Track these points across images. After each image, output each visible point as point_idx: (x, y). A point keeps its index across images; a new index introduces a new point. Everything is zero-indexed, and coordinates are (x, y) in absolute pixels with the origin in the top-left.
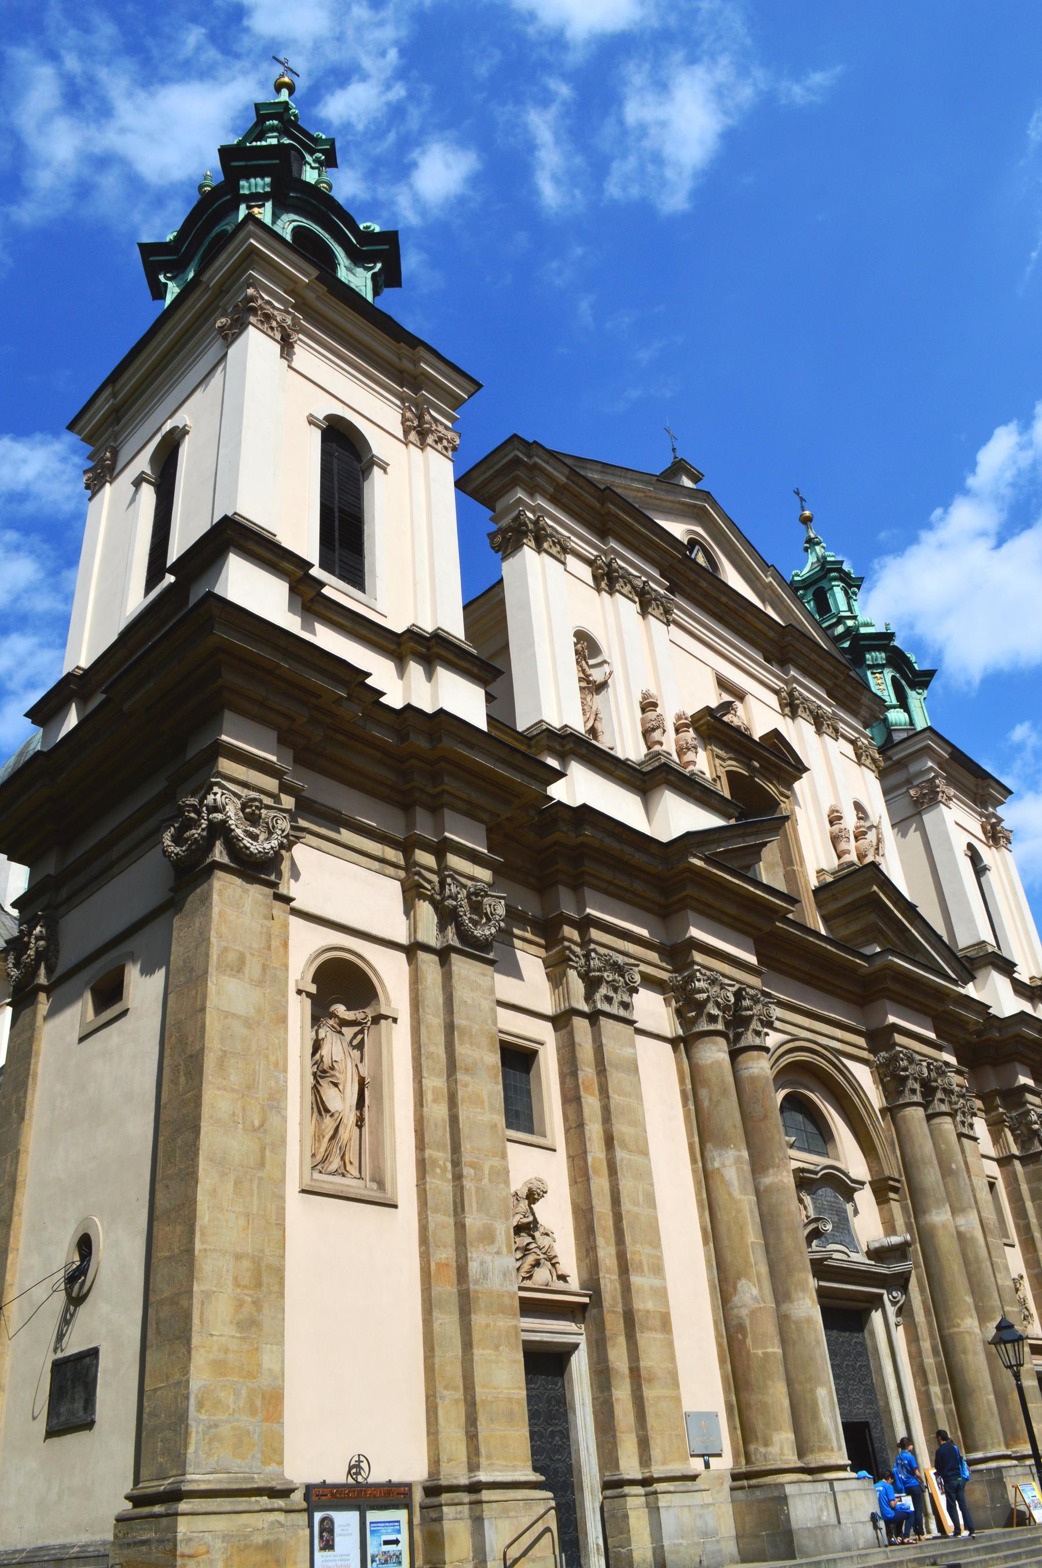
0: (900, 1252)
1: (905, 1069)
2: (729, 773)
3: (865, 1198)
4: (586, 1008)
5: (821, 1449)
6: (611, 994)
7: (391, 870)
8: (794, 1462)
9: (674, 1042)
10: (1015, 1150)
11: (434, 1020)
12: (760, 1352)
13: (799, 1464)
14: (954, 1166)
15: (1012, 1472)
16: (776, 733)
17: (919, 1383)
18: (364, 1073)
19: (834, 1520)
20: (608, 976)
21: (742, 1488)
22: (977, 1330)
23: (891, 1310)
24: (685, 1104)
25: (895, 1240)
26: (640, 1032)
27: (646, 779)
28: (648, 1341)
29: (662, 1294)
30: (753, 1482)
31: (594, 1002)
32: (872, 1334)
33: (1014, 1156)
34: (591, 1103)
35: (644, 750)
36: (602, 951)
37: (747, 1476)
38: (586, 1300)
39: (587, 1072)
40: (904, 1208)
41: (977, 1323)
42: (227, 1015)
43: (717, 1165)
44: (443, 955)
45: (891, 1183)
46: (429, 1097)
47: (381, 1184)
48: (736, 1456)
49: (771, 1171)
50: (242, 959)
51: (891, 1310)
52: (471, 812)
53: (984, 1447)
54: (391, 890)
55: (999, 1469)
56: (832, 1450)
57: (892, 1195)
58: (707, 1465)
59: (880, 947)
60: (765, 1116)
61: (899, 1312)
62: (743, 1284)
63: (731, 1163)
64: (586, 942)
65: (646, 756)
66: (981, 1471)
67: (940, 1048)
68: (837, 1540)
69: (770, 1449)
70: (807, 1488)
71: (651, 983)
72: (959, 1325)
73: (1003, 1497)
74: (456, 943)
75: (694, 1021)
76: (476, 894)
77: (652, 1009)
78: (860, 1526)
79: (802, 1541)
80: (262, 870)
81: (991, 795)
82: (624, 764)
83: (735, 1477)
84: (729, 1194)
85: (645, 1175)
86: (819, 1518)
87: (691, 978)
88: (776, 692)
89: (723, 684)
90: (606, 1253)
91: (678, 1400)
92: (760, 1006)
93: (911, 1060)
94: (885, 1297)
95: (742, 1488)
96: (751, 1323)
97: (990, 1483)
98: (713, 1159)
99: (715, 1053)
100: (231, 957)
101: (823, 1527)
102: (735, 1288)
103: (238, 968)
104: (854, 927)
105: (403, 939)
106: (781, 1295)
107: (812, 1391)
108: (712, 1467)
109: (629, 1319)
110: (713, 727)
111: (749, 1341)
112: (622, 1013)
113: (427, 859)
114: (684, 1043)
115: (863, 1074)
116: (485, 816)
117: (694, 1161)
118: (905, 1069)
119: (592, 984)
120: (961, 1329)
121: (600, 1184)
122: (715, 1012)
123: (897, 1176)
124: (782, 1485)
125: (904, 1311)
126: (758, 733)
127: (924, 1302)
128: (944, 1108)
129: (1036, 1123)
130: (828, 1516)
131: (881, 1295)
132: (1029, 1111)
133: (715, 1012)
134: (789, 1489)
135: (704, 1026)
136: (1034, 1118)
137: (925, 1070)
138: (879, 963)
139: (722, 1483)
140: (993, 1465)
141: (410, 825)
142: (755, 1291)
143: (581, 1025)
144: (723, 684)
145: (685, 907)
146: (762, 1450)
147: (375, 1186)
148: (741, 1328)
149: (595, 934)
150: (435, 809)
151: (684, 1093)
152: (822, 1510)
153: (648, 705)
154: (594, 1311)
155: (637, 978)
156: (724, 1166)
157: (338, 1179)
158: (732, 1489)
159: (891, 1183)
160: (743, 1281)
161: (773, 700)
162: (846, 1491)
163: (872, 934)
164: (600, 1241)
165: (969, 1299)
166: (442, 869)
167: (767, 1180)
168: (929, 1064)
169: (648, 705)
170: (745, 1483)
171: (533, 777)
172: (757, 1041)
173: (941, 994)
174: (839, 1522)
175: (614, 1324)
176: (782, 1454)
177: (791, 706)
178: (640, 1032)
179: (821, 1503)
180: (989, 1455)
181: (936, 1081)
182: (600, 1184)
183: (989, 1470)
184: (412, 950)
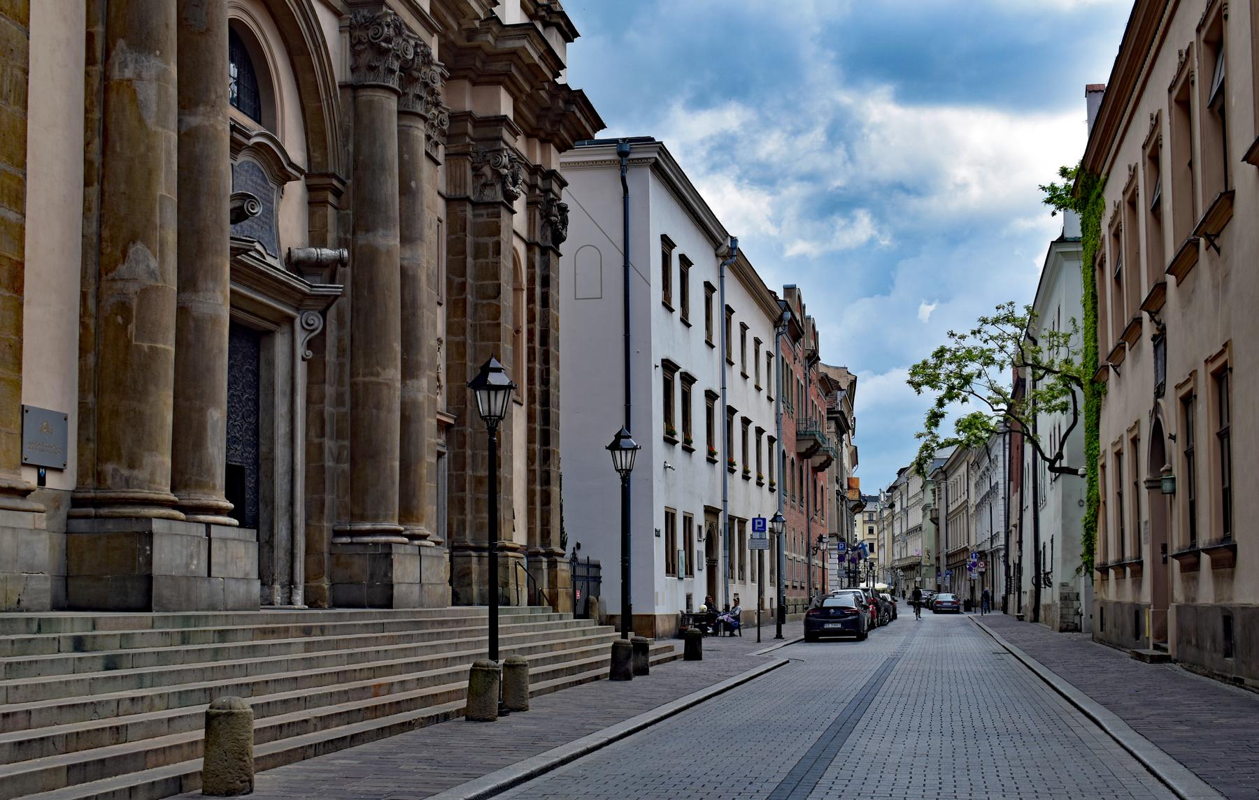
0: (329, 269)
3: (295, 190)
5: (200, 485)
8: (166, 494)
10: (470, 193)
12: (146, 345)
13: (172, 497)
14: (413, 184)
15: (401, 549)
17: (312, 433)
19: (204, 573)
21: (87, 517)
22: (398, 385)
25: (328, 253)
30: (104, 511)
32: (271, 364)
33: (468, 199)
37: (97, 503)
40: (341, 220)
41: (399, 377)
43: (129, 73)
45: (335, 182)
48: (82, 475)
49: (201, 109)
51: (301, 338)
53: (375, 518)
55: (389, 545)
56: (214, 487)
57: (331, 198)
58: (42, 481)
60: (208, 30)
61: (310, 345)
63: (156, 78)
66: (366, 544)
67: (431, 30)
68: (204, 595)
69: (136, 472)
70: (179, 527)
72: (378, 375)
73: (386, 575)
78: (233, 582)
79: (160, 590)
83: (76, 502)
84: (141, 120)
86: (188, 565)
91: (18, 386)
93: (399, 31)
94: (298, 321)
95: (87, 517)
96: (140, 305)
97: (374, 557)
98: (124, 65)
101: (192, 578)
106: (188, 282)
107: (202, 411)
108: (48, 486)
117: (90, 60)
120: (380, 380)
123: (342, 176)
124: (149, 519)
125: (316, 344)
127: (340, 340)
129: (505, 167)
130: (199, 565)
131: (291, 320)
132: (502, 150)
134: (157, 526)
136: (505, 160)
137: (411, 51)
139: (58, 508)
140: (383, 539)
146: (125, 472)
152: (192, 557)
156: (140, 77)
158: (70, 517)
159: (335, 182)
160: (139, 246)
162: (224, 540)
165: (397, 347)
167: (194, 121)
168: (416, 45)
170: (92, 511)
174: (209, 575)
176: (152, 481)
179: (193, 548)
180: (379, 527)
181: (420, 71)
183: (376, 544)
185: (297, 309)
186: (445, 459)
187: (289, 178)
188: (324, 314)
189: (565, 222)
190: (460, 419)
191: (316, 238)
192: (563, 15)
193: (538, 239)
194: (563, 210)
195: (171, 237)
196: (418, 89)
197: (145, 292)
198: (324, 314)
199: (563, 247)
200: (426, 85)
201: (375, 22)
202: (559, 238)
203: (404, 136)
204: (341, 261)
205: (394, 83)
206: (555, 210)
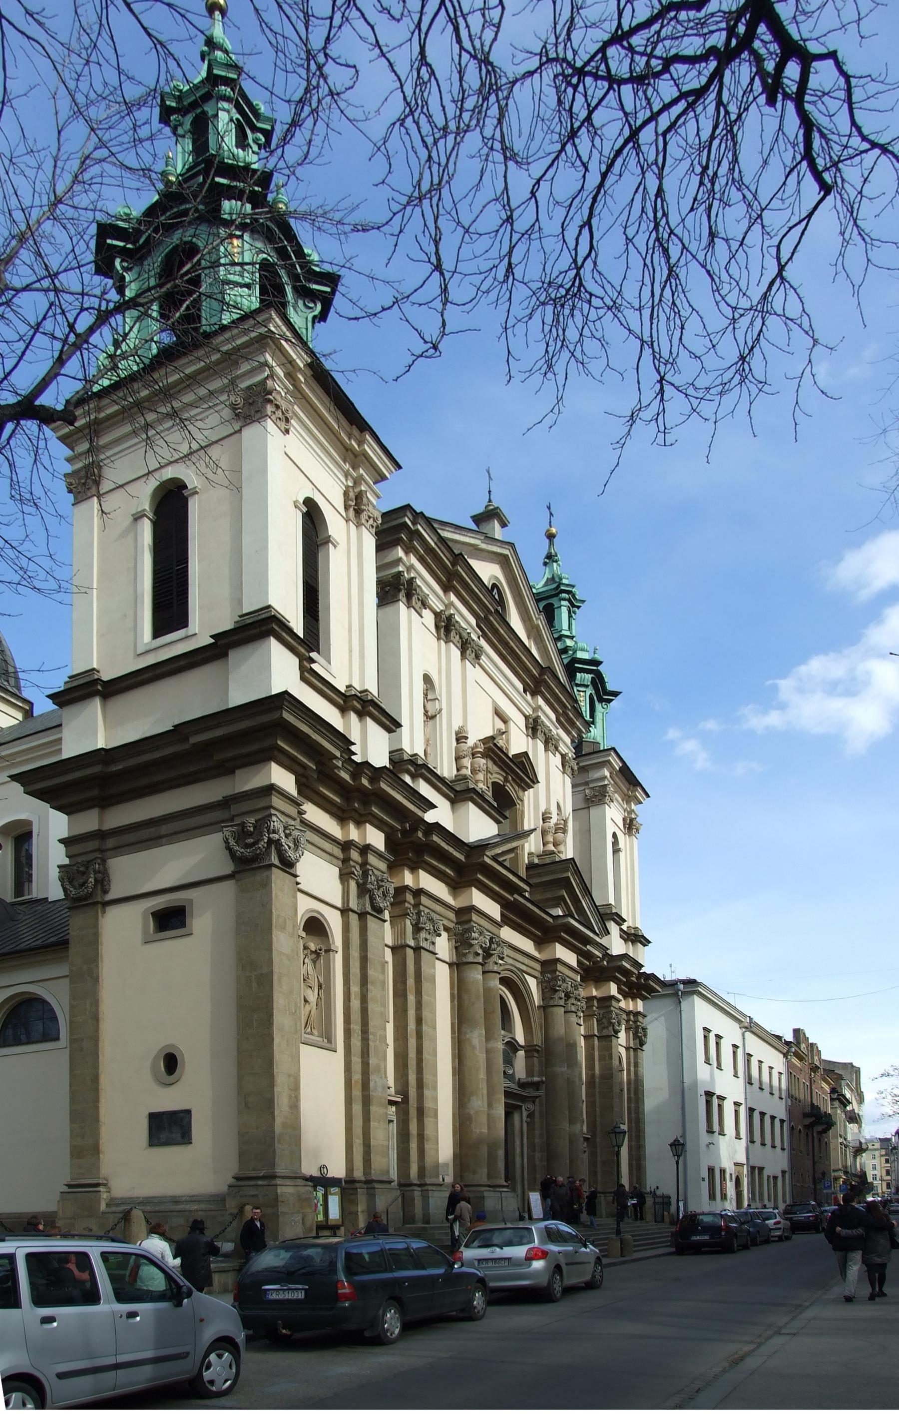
0: (536, 1086)
1: (560, 986)
2: (494, 783)
4: (412, 943)
6: (428, 937)
7: (335, 861)
9: (450, 965)
11: (355, 953)
16: (526, 754)
18: (322, 980)
20: (428, 926)
23: (525, 1114)
24: (452, 1001)
25: (536, 1079)
26: (437, 959)
27: (458, 793)
28: (428, 1121)
29: (435, 1100)
31: (419, 941)
34: (411, 998)
35: (455, 772)
36: (427, 911)
38: (400, 1100)
39: (411, 982)
42: (281, 953)
44: (362, 916)
46: (353, 997)
47: (329, 1041)
50: (285, 922)
52: (380, 825)
54: (334, 871)
59: (563, 911)
62: (474, 1099)
64: (417, 905)
65: (456, 776)
71: (446, 929)
74: (369, 909)
75: (465, 955)
76: (382, 881)
77: (443, 945)
80: (288, 865)
81: (636, 797)
82: (442, 780)
85: (434, 1040)
87: (470, 930)
88: (527, 718)
89: (498, 713)
90: (412, 1078)
92: (499, 948)
93: (564, 981)
99: (476, 975)
100: (281, 920)
102: (469, 1100)
103: (283, 928)
104: (549, 895)
105: (339, 904)
106: (490, 1105)
109: (421, 1112)
110: (492, 749)
111: (473, 1126)
112: (431, 949)
113: (355, 855)
114: (458, 966)
115: (532, 983)
116: (386, 829)
118: (560, 986)
119: (417, 929)
121: (412, 1042)
122: (480, 951)
126: (514, 750)
128: (573, 1009)
133: (480, 951)
135: (471, 958)
138: (560, 921)
141: (346, 831)
142: (480, 1103)
143: (410, 953)
144: (498, 713)
145: (470, 886)
147: (326, 1041)
148: (469, 1118)
149: (424, 900)
150: (359, 824)
151: (452, 995)
153: (461, 738)
154: (402, 1106)
155: (442, 928)
157: (310, 1037)
161: (521, 722)
163: (558, 901)
164: (410, 1072)
166: (364, 864)
169: (461, 738)
171: (419, 808)
172: (496, 968)
173: (587, 941)
175: (413, 1113)
177: (534, 727)
178: (437, 959)
182: (412, 1042)
184: (345, 911)
185: (523, 1102)
186: (587, 1153)
187: (518, 1050)
188: (534, 1102)
189: (645, 1035)
190: (594, 1135)
191: (529, 1071)
192: (643, 936)
193: (632, 1045)
194: (644, 1029)
195: (485, 1092)
196: (572, 1001)
197: (477, 1112)
198: (534, 1102)
199: (644, 1047)
200: (576, 998)
201: (556, 979)
202: (642, 1044)
203: (567, 1022)
204: (542, 1082)
205: (562, 1002)
206: (640, 1030)
